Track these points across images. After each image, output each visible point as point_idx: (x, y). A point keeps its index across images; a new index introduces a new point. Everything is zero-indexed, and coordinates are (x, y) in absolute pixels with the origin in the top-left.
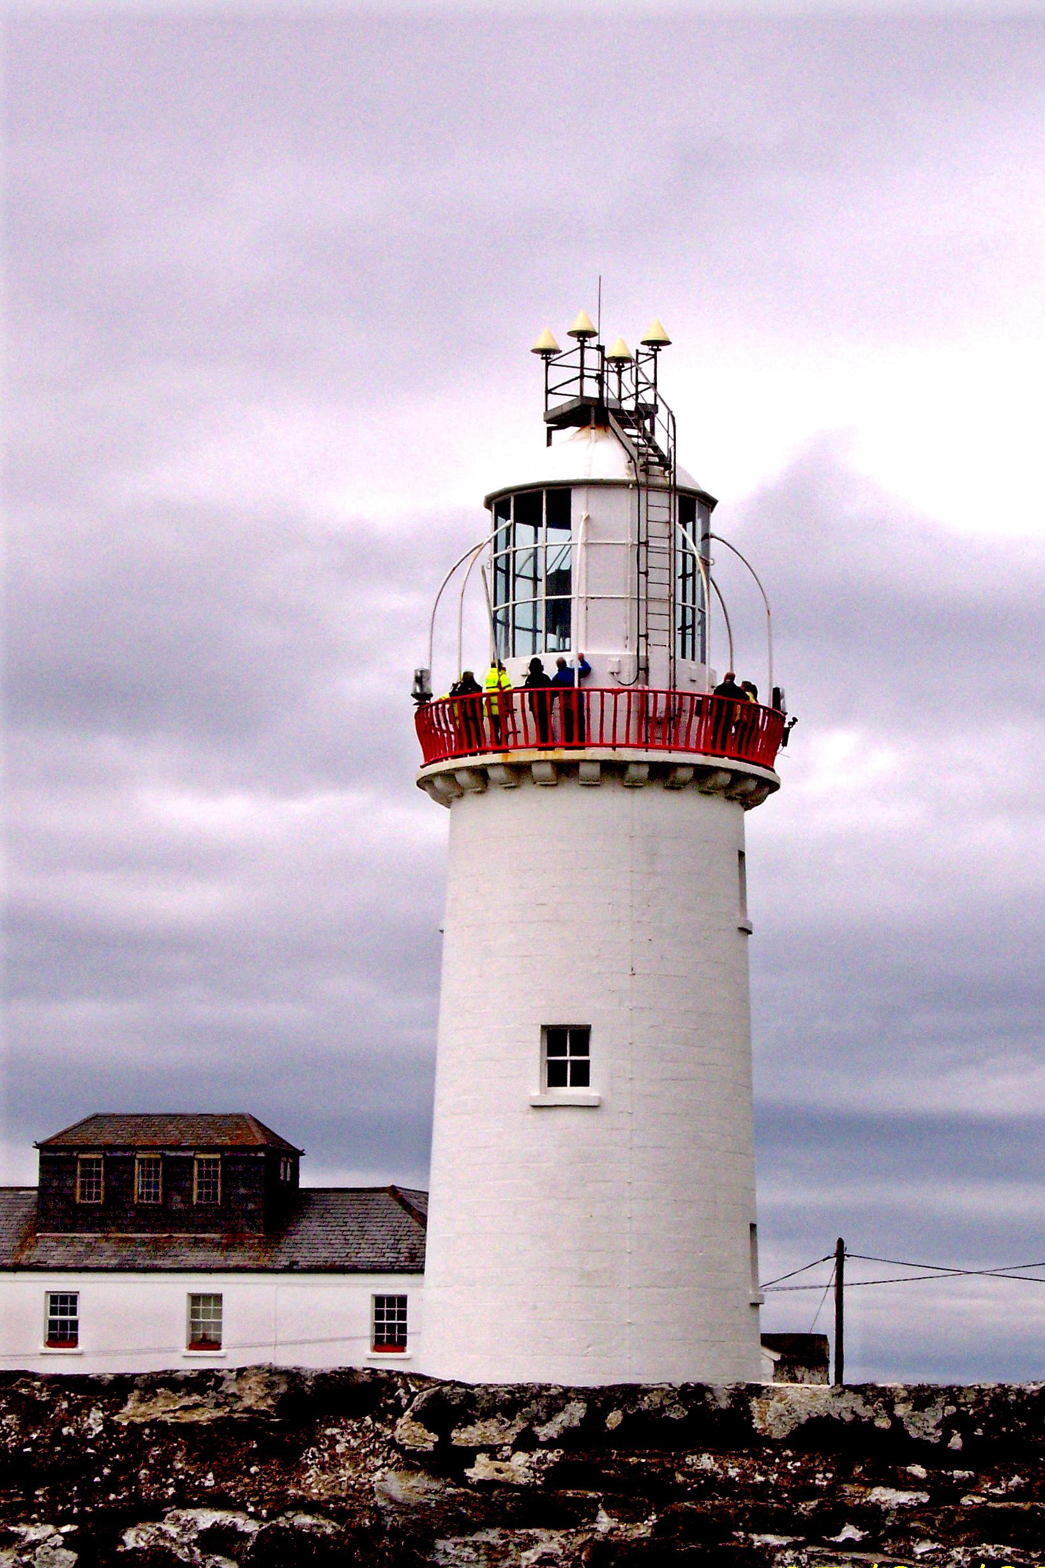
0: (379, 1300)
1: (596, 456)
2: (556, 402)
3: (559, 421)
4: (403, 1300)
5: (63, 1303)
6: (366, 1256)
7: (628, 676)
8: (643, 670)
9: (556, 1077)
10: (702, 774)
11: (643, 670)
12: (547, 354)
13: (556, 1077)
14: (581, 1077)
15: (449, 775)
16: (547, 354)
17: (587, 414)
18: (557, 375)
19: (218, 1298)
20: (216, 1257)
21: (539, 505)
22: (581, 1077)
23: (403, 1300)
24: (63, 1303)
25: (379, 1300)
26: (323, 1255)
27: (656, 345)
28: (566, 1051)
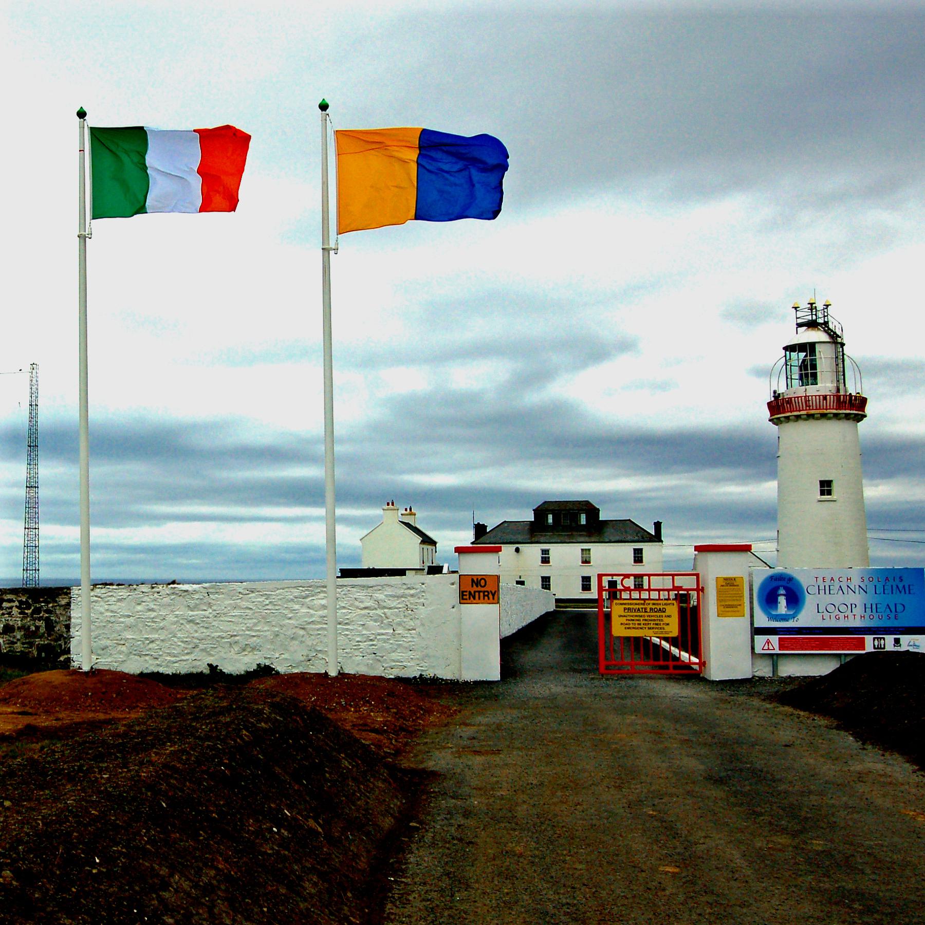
0: (635, 550)
1: (817, 336)
2: (799, 321)
3: (799, 325)
4: (641, 550)
5: (545, 552)
6: (629, 538)
7: (834, 391)
8: (838, 390)
9: (822, 493)
10: (847, 415)
11: (838, 390)
12: (796, 308)
13: (822, 493)
14: (829, 493)
15: (778, 419)
16: (796, 308)
17: (812, 325)
18: (799, 314)
19: (589, 550)
20: (587, 539)
21: (809, 348)
22: (829, 493)
23: (641, 550)
24: (545, 552)
25: (635, 550)
26: (617, 538)
27: (827, 306)
28: (826, 487)
